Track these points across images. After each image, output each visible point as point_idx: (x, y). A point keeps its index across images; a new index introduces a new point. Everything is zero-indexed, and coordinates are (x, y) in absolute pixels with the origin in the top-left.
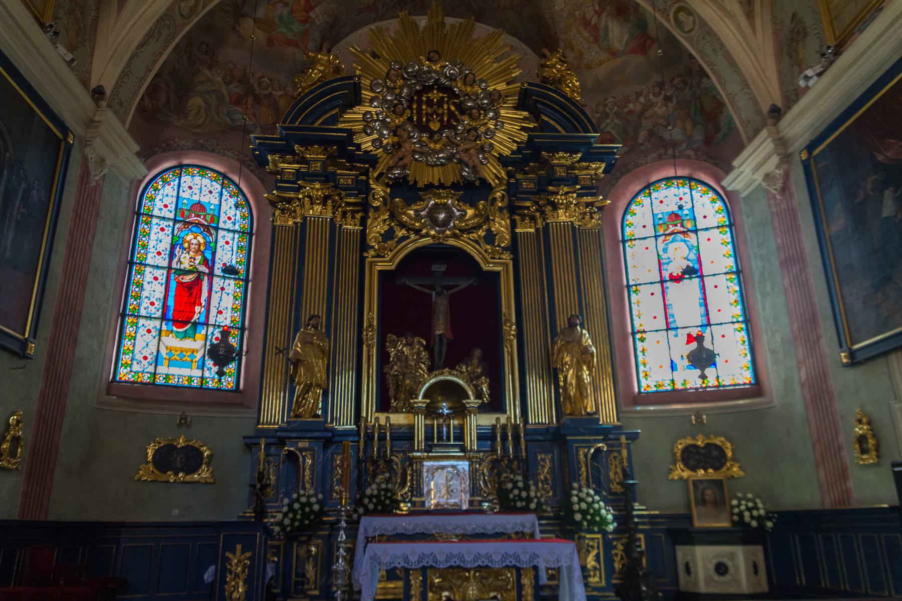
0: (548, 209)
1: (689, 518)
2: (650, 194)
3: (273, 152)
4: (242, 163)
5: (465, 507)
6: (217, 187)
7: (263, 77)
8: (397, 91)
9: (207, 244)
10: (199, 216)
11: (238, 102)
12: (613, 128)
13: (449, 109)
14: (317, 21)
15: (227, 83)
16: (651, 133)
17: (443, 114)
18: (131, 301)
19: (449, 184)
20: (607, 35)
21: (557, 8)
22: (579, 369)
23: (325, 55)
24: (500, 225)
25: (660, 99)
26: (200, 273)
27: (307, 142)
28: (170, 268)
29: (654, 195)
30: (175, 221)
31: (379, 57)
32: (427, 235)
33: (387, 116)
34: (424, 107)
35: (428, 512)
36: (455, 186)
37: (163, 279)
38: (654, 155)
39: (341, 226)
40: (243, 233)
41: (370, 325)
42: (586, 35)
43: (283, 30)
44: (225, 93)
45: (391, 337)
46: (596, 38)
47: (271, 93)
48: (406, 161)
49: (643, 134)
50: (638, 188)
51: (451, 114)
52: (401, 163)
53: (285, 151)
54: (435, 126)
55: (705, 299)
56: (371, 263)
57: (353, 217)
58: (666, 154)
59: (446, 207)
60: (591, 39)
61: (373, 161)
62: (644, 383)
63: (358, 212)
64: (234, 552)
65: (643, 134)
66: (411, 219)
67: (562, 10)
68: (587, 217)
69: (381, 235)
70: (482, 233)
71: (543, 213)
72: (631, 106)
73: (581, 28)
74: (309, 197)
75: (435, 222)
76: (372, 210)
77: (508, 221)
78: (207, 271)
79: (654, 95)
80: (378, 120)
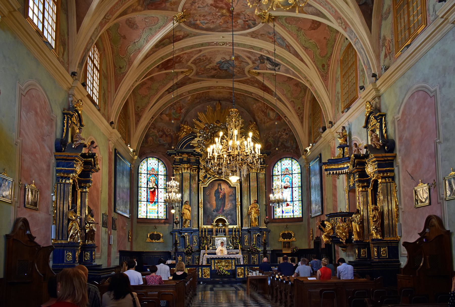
8: (207, 133)
11: (161, 137)
15: (158, 132)
16: (282, 144)
20: (269, 114)
31: (201, 122)
32: (216, 177)
33: (204, 142)
41: (201, 202)
43: (174, 116)
47: (170, 134)
49: (280, 143)
50: (278, 160)
57: (195, 171)
65: (280, 143)
66: (212, 172)
68: (262, 170)
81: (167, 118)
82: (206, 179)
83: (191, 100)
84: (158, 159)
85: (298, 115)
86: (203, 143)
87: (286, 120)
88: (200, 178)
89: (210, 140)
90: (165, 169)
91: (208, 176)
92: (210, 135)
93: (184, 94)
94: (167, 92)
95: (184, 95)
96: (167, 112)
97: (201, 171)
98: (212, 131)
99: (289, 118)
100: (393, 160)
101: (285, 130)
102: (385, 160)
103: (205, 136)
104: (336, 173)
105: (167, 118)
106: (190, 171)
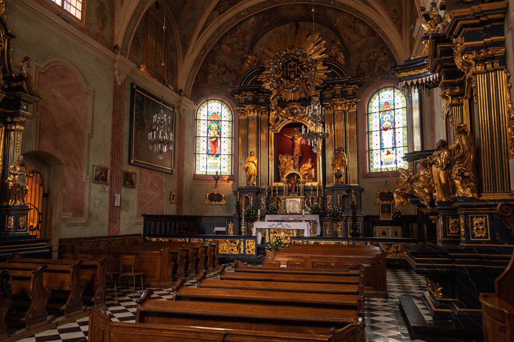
1: (379, 216)
2: (379, 94)
3: (236, 94)
4: (227, 96)
6: (220, 105)
7: (231, 63)
9: (218, 127)
10: (215, 117)
11: (224, 73)
12: (365, 67)
13: (297, 68)
14: (248, 40)
15: (219, 68)
16: (379, 68)
17: (295, 71)
18: (197, 149)
21: (337, 22)
23: (250, 56)
25: (382, 54)
26: (217, 138)
27: (246, 91)
28: (207, 137)
29: (380, 94)
30: (208, 120)
31: (271, 50)
32: (290, 119)
33: (274, 75)
34: (288, 69)
36: (299, 101)
37: (206, 141)
38: (379, 78)
39: (261, 118)
40: (230, 121)
42: (351, 31)
43: (237, 46)
45: (280, 155)
46: (355, 32)
48: (281, 93)
49: (376, 68)
50: (375, 91)
51: (298, 70)
52: (279, 94)
53: (239, 93)
54: (292, 76)
55: (395, 138)
57: (265, 114)
58: (384, 77)
59: (296, 109)
60: (353, 32)
61: (271, 93)
62: (371, 169)
63: (267, 111)
64: (230, 224)
65: (376, 68)
66: (284, 114)
67: (339, 23)
69: (275, 120)
72: (371, 57)
73: (348, 28)
74: (249, 110)
75: (293, 114)
76: (271, 111)
78: (219, 136)
79: (380, 52)
81: (229, 49)
82: (277, 122)
83: (255, 23)
84: (222, 101)
85: (395, 22)
86: (273, 77)
87: (379, 32)
88: (271, 122)
89: (282, 72)
90: (230, 113)
91: (280, 118)
92: (281, 65)
93: (242, 14)
94: (216, 13)
95: (244, 16)
96: (228, 42)
97: (271, 113)
98: (285, 60)
99: (382, 29)
100: (502, 20)
101: (382, 49)
102: (482, 24)
104: (417, 83)
105: (229, 49)
106: (258, 114)
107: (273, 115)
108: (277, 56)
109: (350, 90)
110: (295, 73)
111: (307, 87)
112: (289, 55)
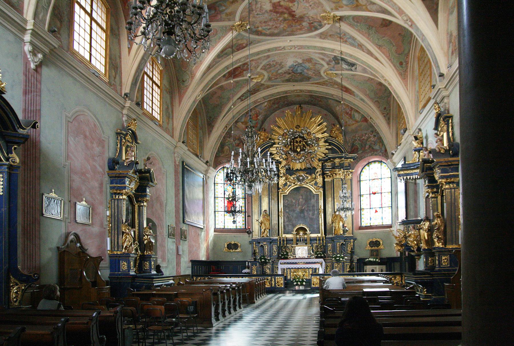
0: (334, 175)
5: (306, 257)
16: (370, 146)
19: (303, 169)
22: (339, 222)
24: (320, 180)
28: (224, 197)
32: (296, 185)
35: (297, 259)
36: (305, 169)
38: (370, 154)
42: (347, 116)
44: (234, 143)
46: (351, 117)
48: (289, 163)
49: (367, 146)
51: (304, 146)
54: (299, 150)
56: (281, 193)
65: (367, 146)
70: (313, 182)
71: (333, 175)
72: (364, 137)
75: (299, 180)
77: (322, 178)
79: (371, 134)
80: (281, 149)
86: (282, 150)
88: (280, 187)
89: (290, 147)
91: (288, 183)
97: (280, 179)
98: (292, 137)
101: (372, 132)
103: (284, 141)
107: (282, 181)
108: (285, 133)
109: (347, 162)
110: (301, 147)
111: (311, 159)
112: (296, 132)
